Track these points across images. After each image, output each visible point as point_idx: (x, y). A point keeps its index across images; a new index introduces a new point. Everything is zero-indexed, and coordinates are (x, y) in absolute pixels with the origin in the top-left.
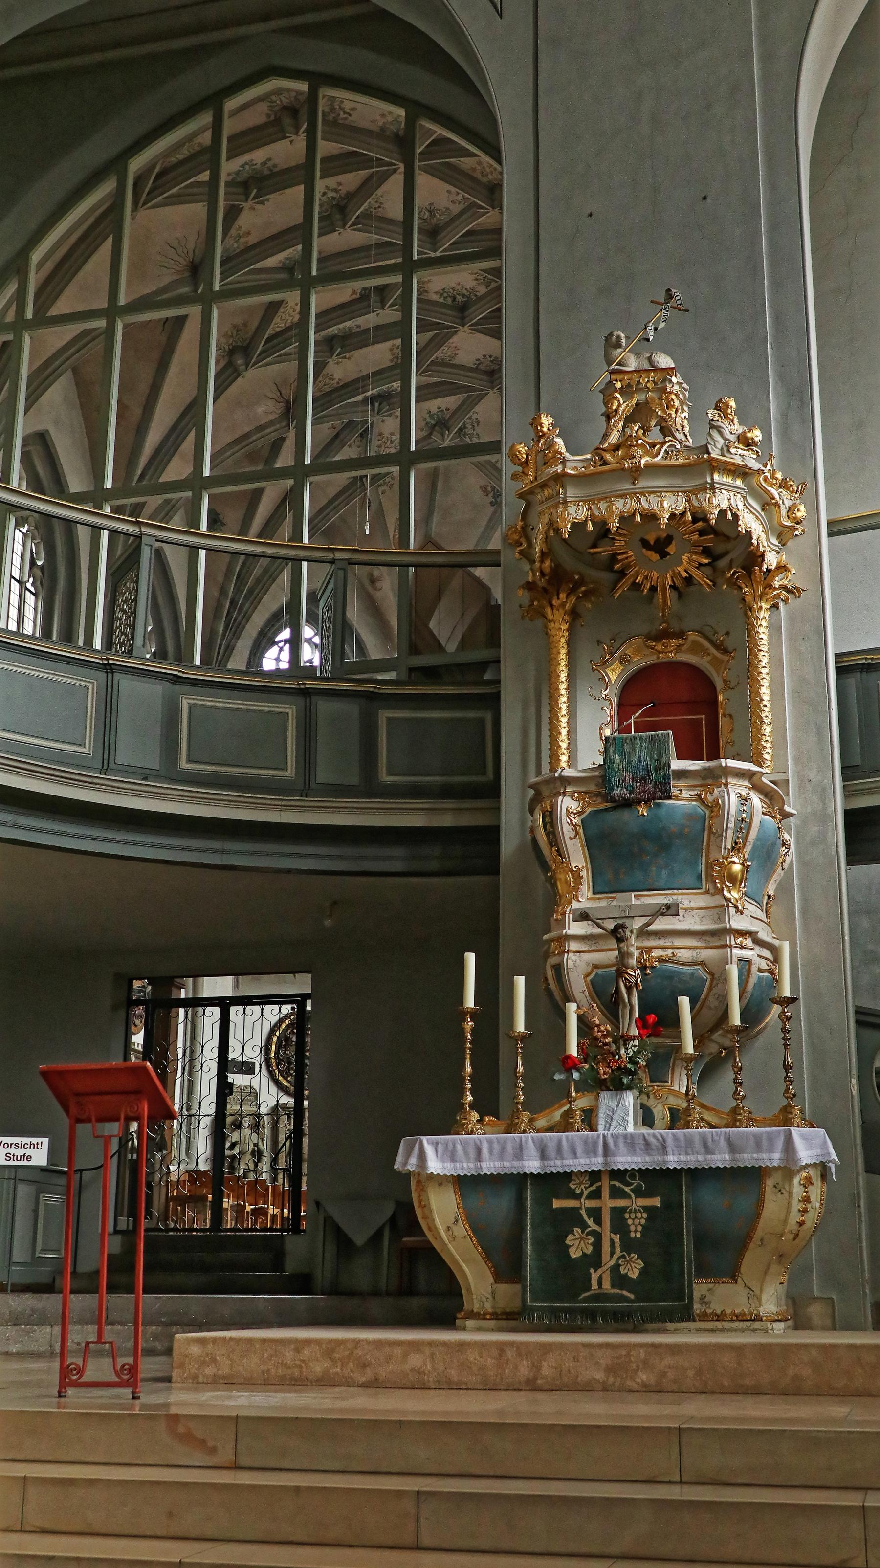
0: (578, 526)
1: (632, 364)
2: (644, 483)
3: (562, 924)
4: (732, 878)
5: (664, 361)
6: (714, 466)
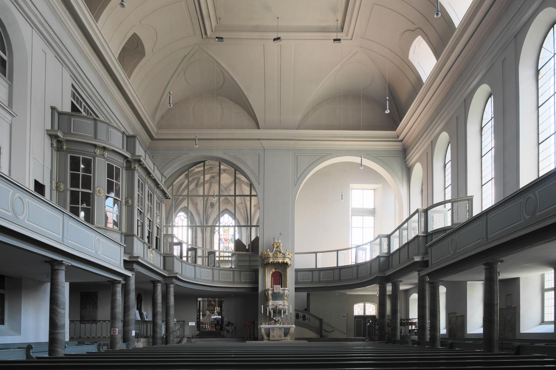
0: (271, 262)
1: (277, 241)
2: (278, 258)
3: (269, 303)
4: (286, 300)
5: (280, 241)
6: (286, 257)
